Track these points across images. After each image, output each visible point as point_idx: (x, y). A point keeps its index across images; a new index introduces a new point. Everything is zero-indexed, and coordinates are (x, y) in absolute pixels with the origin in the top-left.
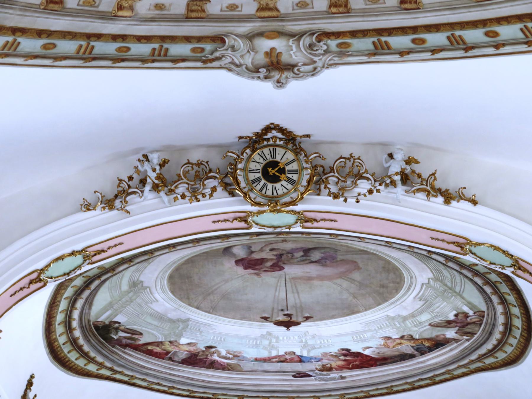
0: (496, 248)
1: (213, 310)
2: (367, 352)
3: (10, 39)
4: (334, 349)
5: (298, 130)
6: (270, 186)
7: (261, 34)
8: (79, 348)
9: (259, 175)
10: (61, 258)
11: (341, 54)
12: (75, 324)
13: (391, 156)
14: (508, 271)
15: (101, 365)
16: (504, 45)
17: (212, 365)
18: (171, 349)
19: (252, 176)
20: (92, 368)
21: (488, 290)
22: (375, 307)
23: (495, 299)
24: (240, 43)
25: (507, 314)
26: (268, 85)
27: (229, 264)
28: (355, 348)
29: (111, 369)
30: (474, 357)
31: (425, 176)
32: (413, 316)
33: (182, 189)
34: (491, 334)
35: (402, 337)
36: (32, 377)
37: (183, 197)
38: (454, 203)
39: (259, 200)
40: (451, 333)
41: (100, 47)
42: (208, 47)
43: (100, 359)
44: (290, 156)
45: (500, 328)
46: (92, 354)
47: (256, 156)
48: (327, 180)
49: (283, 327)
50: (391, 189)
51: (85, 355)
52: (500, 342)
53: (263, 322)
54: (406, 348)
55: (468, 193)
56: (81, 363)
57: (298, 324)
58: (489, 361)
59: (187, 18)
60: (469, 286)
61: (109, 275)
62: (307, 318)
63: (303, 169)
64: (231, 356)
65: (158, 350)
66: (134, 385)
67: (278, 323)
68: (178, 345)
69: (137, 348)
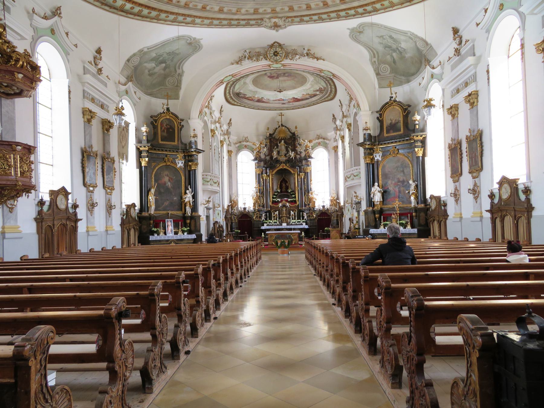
0: (329, 71)
1: (263, 89)
2: (298, 98)
3: (211, 21)
4: (291, 97)
5: (282, 43)
6: (275, 57)
7: (272, 18)
8: (232, 99)
9: (273, 55)
10: (227, 77)
11: (292, 22)
12: (231, 93)
13: (304, 49)
14: (331, 77)
15: (238, 103)
16: (332, 19)
17: (263, 102)
18: (254, 98)
19: (271, 55)
20: (236, 103)
21: (327, 82)
23: (328, 84)
24: (267, 20)
25: (331, 88)
26: (274, 32)
27: (266, 77)
28: (296, 97)
29: (240, 103)
30: (323, 98)
31: (312, 54)
32: (309, 89)
33: (254, 59)
34: (327, 93)
35: (307, 94)
36: (222, 106)
37: (255, 61)
38: (319, 60)
39: (273, 61)
40: (318, 93)
41: (234, 22)
42: (259, 21)
43: (237, 101)
44: (280, 49)
45: (329, 91)
46: (236, 100)
47: (272, 50)
48: (289, 56)
50: (304, 57)
51: (234, 100)
52: (329, 95)
54: (308, 96)
55: (323, 58)
56: (233, 102)
57: (282, 91)
58: (327, 99)
59: (254, 14)
60: (322, 81)
62: (285, 90)
63: (283, 53)
65: (250, 99)
66: (245, 107)
67: (278, 91)
68: (255, 97)
69: (246, 98)
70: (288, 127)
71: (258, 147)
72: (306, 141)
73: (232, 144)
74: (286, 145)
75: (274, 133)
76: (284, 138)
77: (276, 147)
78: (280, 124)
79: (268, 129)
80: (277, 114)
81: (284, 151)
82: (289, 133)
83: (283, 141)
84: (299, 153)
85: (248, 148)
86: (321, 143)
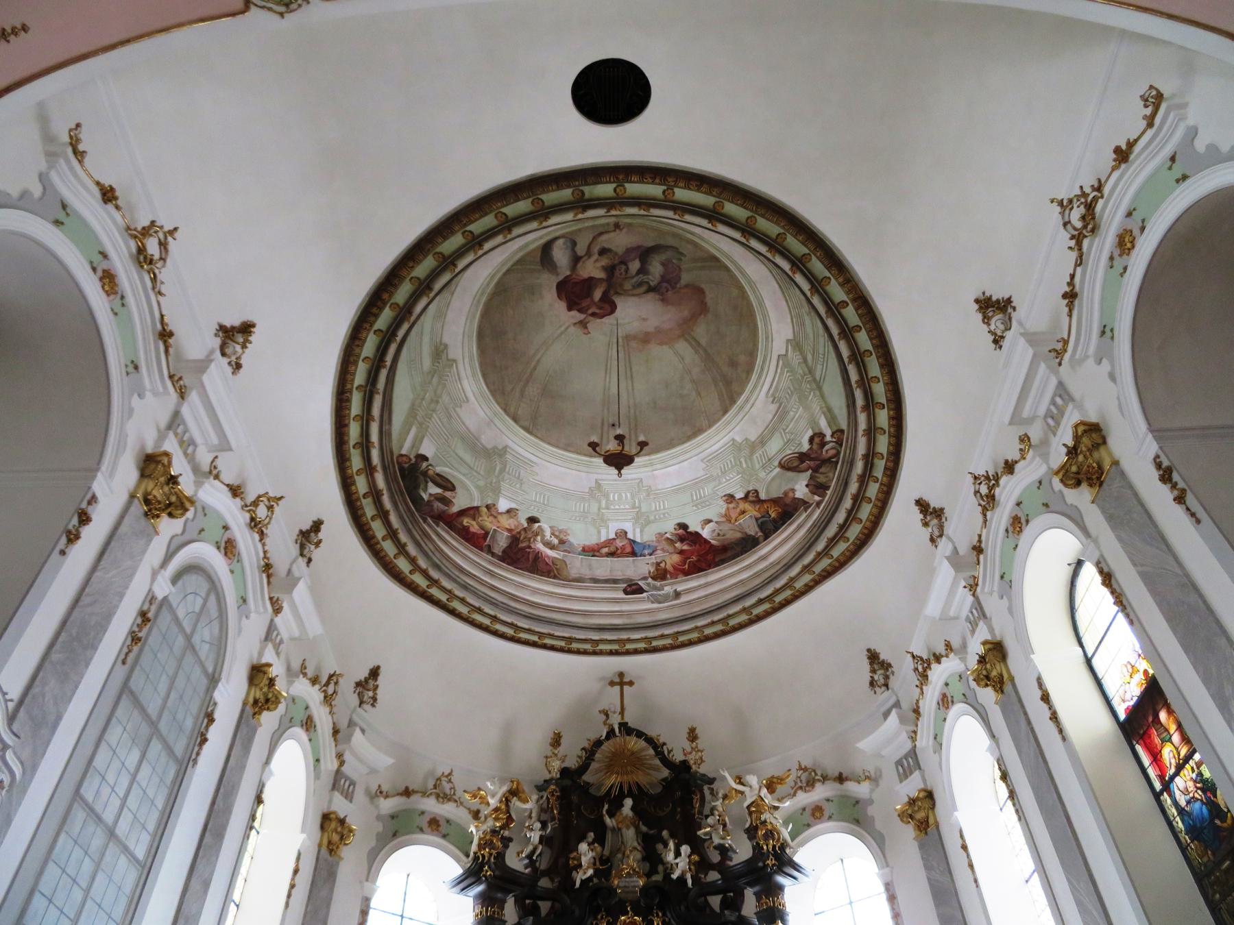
22: (719, 420)
34: (846, 484)
49: (613, 468)
53: (591, 456)
61: (405, 326)
64: (556, 541)
70: (651, 732)
71: (497, 810)
72: (753, 780)
73: (359, 795)
74: (644, 829)
75: (584, 768)
76: (635, 789)
77: (591, 835)
78: (615, 720)
79: (556, 741)
80: (602, 679)
81: (633, 860)
82: (657, 762)
83: (628, 802)
84: (715, 857)
85: (444, 836)
86: (828, 809)
